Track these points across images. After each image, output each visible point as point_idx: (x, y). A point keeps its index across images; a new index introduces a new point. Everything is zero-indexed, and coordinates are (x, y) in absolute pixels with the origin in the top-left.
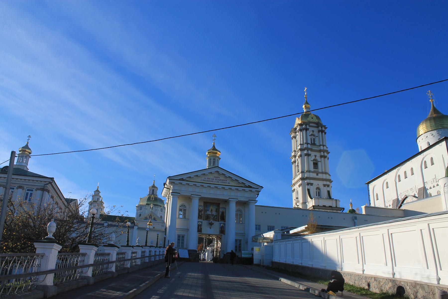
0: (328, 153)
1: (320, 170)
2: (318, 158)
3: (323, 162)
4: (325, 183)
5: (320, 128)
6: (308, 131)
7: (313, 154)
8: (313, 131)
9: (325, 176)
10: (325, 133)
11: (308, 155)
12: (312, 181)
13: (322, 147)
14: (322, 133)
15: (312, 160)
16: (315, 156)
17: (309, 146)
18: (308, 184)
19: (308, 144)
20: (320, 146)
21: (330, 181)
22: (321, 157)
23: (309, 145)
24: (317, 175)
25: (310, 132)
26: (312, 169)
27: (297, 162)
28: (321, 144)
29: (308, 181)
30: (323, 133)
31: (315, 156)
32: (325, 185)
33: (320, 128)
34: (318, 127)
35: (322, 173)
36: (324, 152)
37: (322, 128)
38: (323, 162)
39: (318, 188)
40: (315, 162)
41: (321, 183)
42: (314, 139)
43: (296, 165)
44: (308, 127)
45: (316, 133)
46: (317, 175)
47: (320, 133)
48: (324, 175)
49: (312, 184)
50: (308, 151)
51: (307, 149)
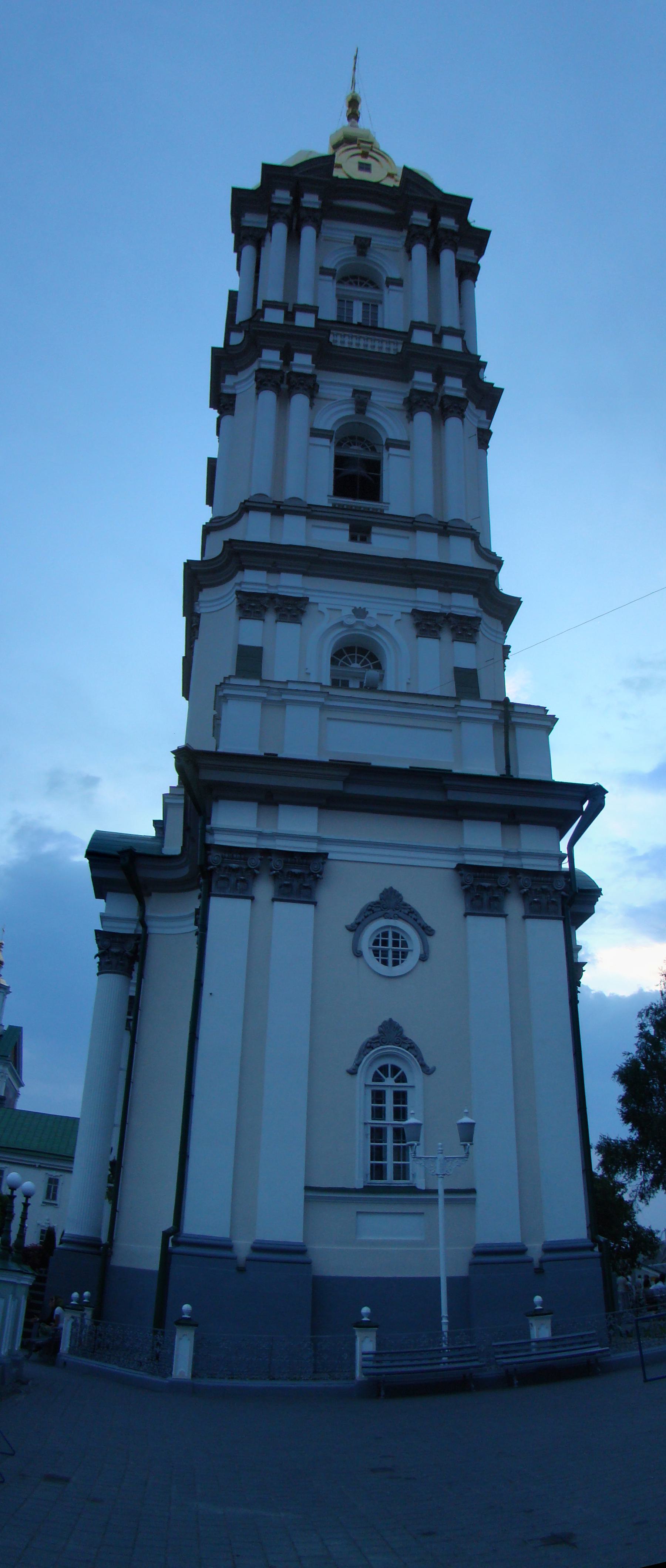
2: (391, 426)
4: (430, 599)
6: (308, 233)
8: (362, 245)
11: (283, 384)
12: (290, 584)
15: (328, 420)
16: (361, 399)
18: (252, 605)
22: (414, 404)
24: (360, 533)
28: (422, 315)
29: (255, 580)
31: (361, 399)
32: (427, 624)
35: (411, 525)
40: (355, 451)
46: (360, 533)
49: (292, 609)
51: (288, 339)
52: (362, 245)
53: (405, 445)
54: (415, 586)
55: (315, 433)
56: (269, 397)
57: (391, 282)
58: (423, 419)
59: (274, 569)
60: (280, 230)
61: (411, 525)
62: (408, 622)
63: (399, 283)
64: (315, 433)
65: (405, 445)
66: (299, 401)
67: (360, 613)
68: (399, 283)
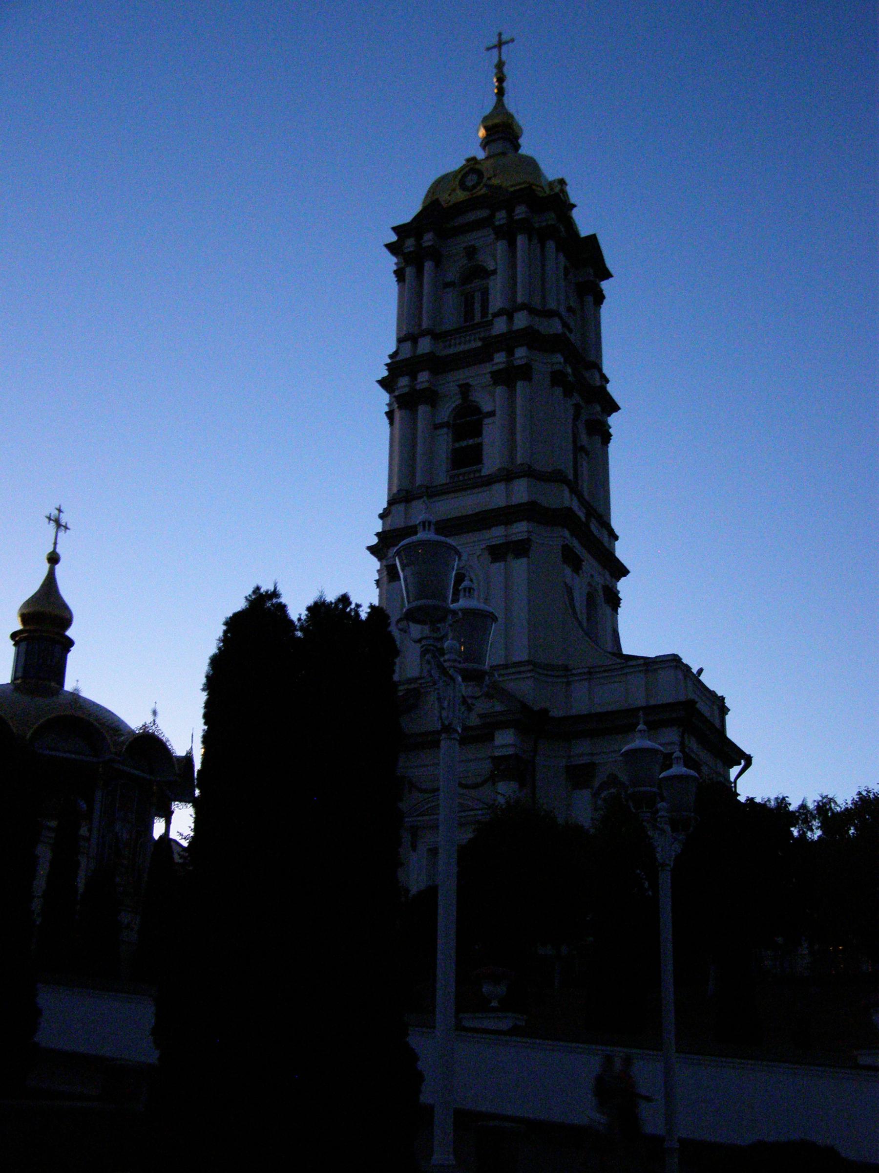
43: (445, 412)
47: (590, 299)
48: (605, 533)
49: (576, 564)
54: (604, 567)
58: (598, 439)
60: (551, 245)
65: (587, 454)
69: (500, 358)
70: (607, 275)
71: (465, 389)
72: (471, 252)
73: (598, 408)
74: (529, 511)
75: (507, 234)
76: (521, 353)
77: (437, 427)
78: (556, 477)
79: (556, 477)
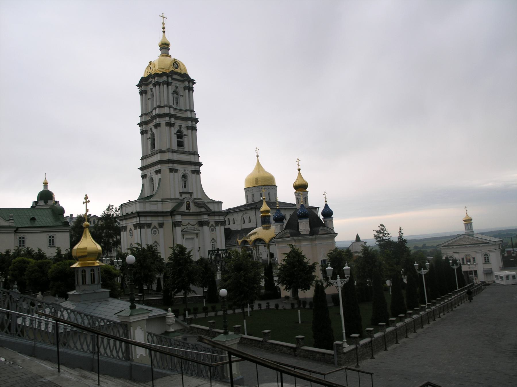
0: (196, 121)
1: (186, 150)
3: (190, 135)
4: (193, 168)
5: (187, 84)
7: (178, 123)
8: (177, 87)
9: (192, 158)
10: (193, 91)
12: (176, 166)
13: (189, 113)
14: (189, 91)
17: (172, 111)
18: (171, 170)
19: (170, 107)
20: (186, 110)
21: (200, 164)
22: (188, 128)
23: (172, 109)
25: (171, 89)
26: (175, 147)
27: (149, 133)
28: (188, 108)
29: (171, 166)
30: (191, 92)
33: (187, 84)
34: (183, 81)
35: (189, 153)
36: (192, 121)
37: (189, 83)
38: (190, 135)
39: (184, 177)
41: (188, 169)
42: (177, 99)
43: (149, 135)
44: (170, 79)
45: (181, 91)
47: (187, 91)
48: (192, 156)
49: (176, 171)
50: (170, 118)
52: (177, 87)
53: (187, 135)
55: (175, 134)
56: (168, 128)
57: (181, 96)
59: (173, 163)
60: (165, 86)
61: (189, 153)
62: (190, 172)
63: (182, 96)
64: (175, 134)
65: (187, 135)
66: (172, 128)
67: (185, 170)
68: (182, 96)
69: (154, 121)
70: (193, 82)
71: (151, 129)
72: (151, 89)
73: (190, 122)
74: (161, 162)
75: (155, 85)
76: (158, 119)
77: (148, 139)
78: (168, 151)
79: (168, 151)
